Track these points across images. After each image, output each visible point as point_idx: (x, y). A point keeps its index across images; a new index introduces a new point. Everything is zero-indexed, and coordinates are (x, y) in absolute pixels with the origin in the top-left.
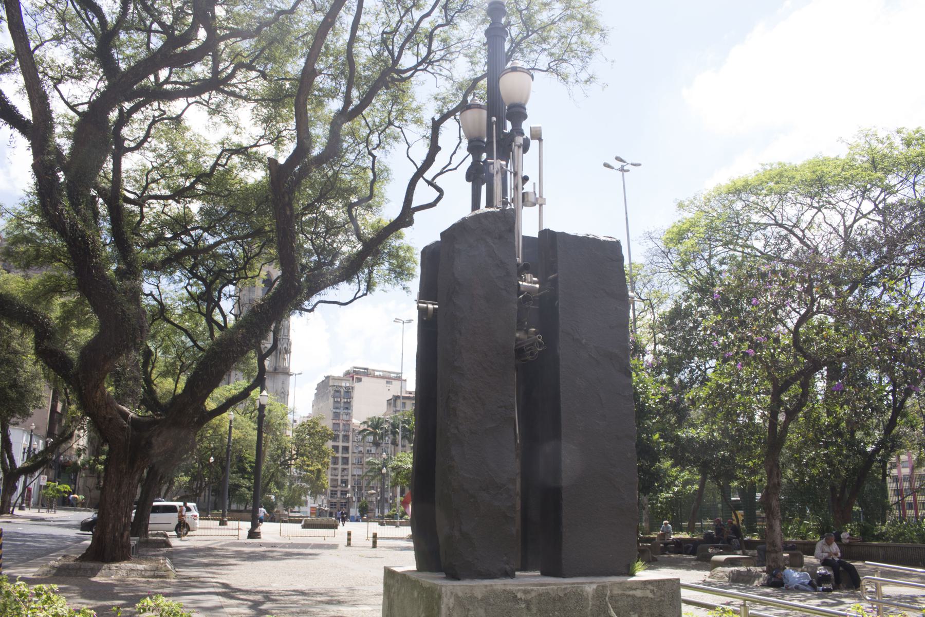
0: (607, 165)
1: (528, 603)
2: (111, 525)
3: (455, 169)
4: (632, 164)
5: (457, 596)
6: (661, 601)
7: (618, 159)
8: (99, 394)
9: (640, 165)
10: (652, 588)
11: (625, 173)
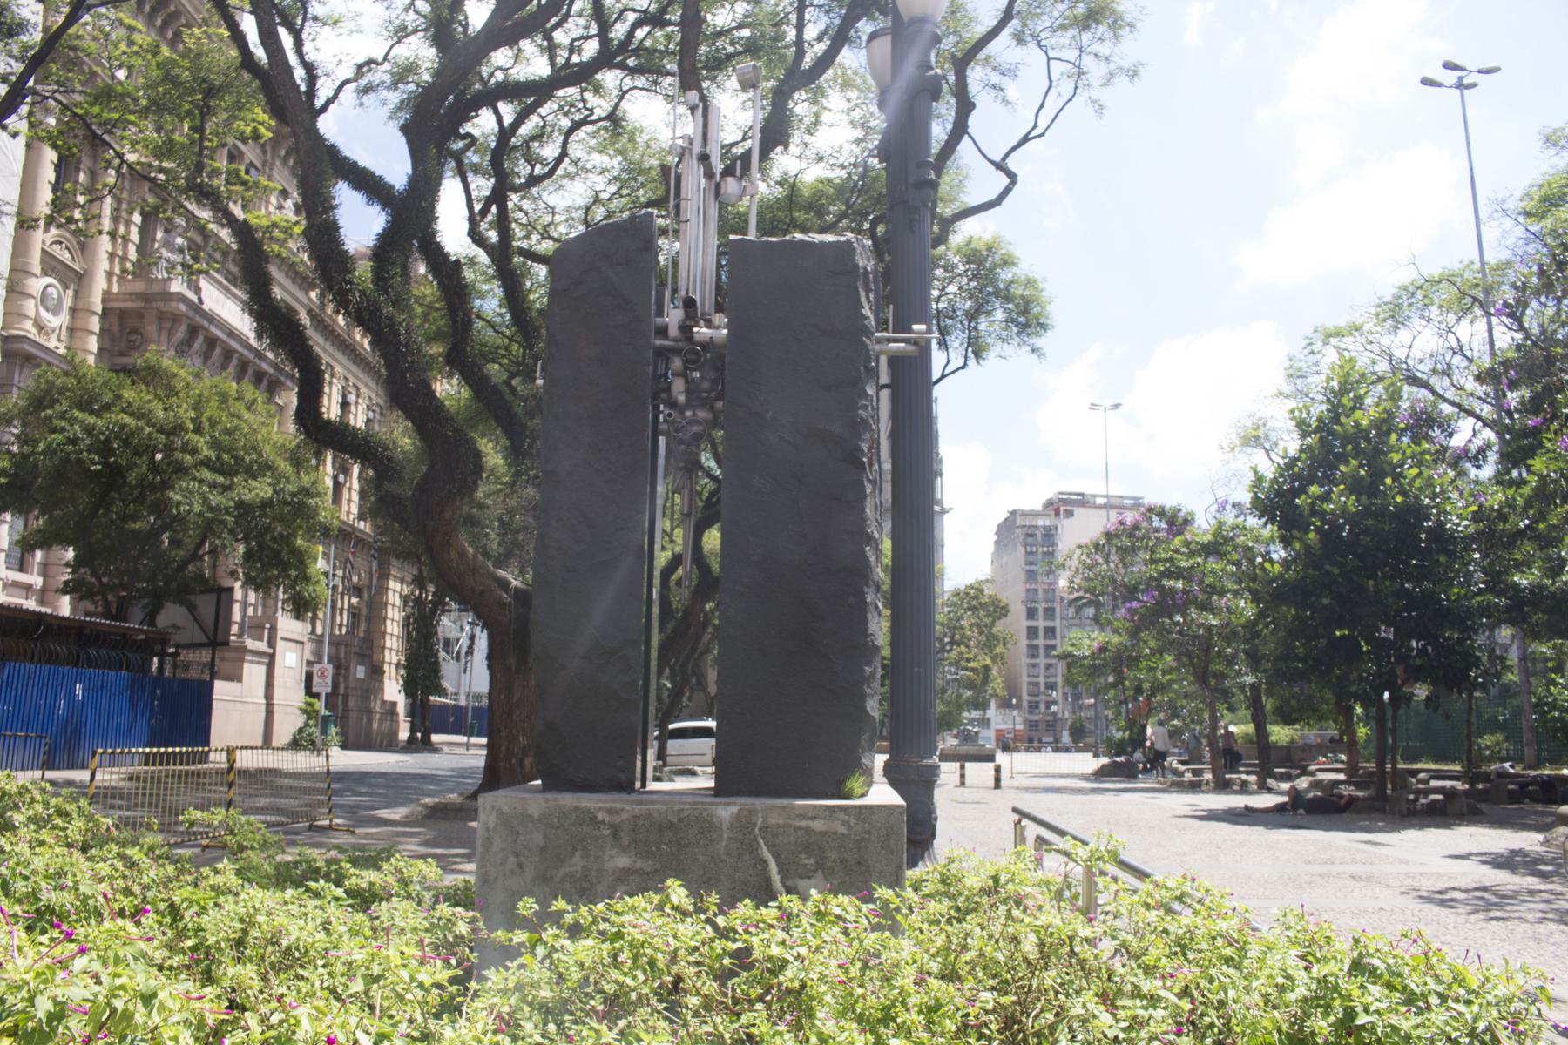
0: (1427, 82)
1: (615, 830)
2: (503, 748)
3: (1042, 135)
4: (1480, 72)
5: (500, 813)
6: (863, 840)
7: (1448, 66)
8: (453, 555)
9: (1497, 69)
10: (846, 818)
11: (1466, 92)
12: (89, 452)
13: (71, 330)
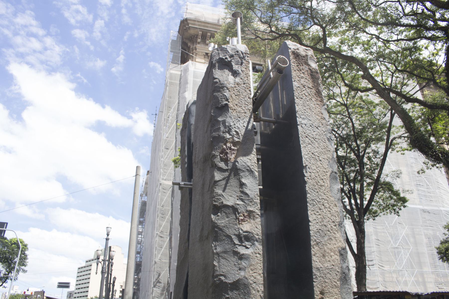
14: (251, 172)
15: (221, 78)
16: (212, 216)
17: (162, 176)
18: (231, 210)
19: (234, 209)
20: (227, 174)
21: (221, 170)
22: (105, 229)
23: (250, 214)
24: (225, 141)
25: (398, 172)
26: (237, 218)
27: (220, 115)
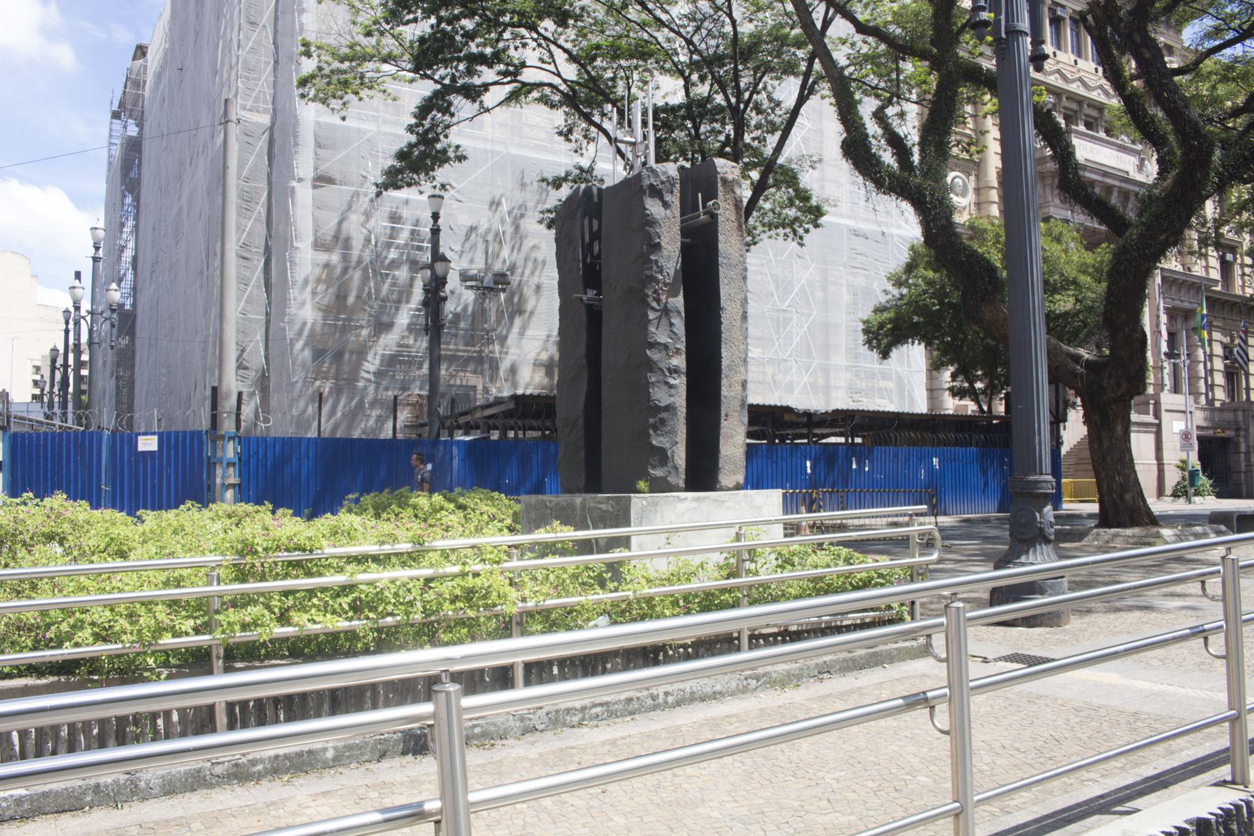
12: (931, 298)
13: (978, 205)
14: (679, 312)
15: (652, 209)
16: (648, 352)
17: (241, 99)
18: (663, 347)
19: (666, 347)
20: (658, 314)
21: (653, 309)
22: (89, 233)
23: (678, 351)
24: (658, 281)
25: (814, 159)
26: (668, 354)
27: (652, 253)
